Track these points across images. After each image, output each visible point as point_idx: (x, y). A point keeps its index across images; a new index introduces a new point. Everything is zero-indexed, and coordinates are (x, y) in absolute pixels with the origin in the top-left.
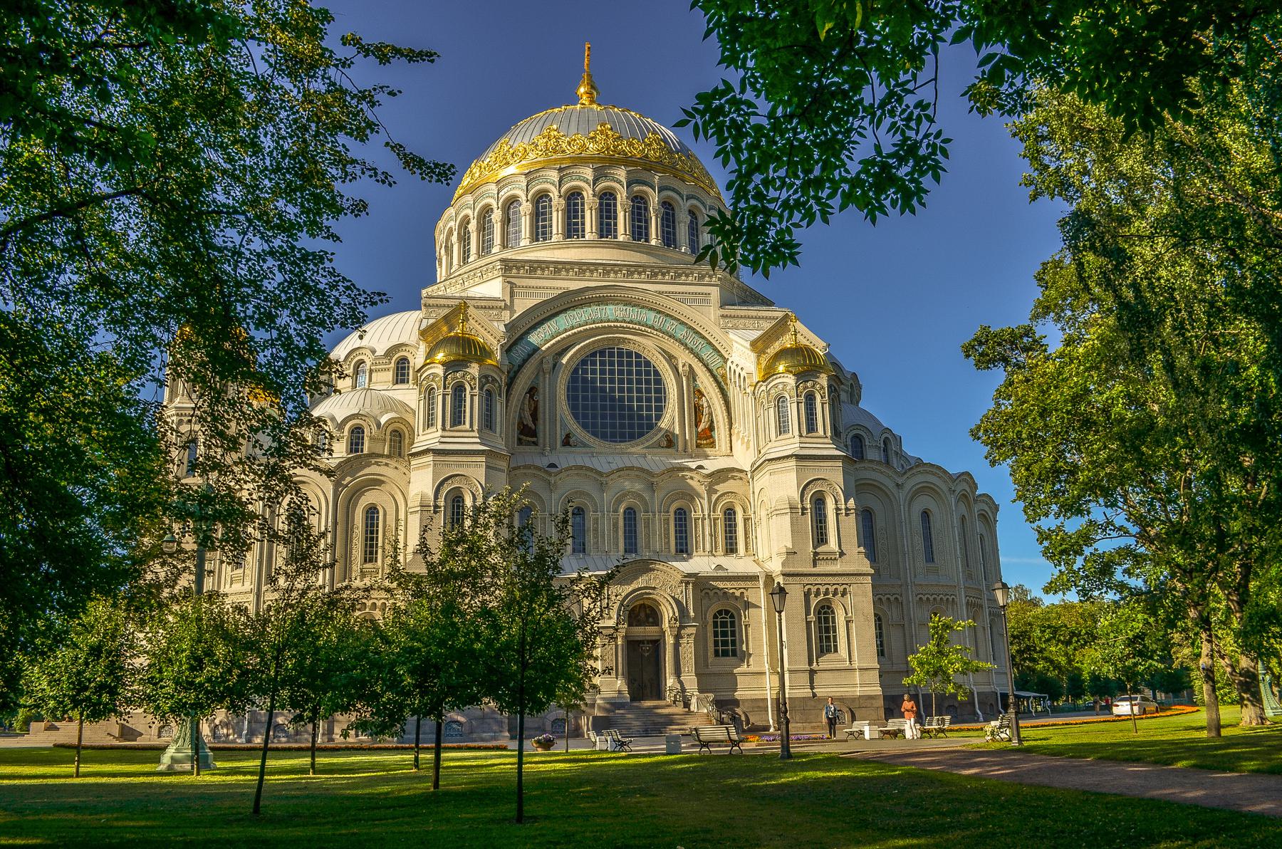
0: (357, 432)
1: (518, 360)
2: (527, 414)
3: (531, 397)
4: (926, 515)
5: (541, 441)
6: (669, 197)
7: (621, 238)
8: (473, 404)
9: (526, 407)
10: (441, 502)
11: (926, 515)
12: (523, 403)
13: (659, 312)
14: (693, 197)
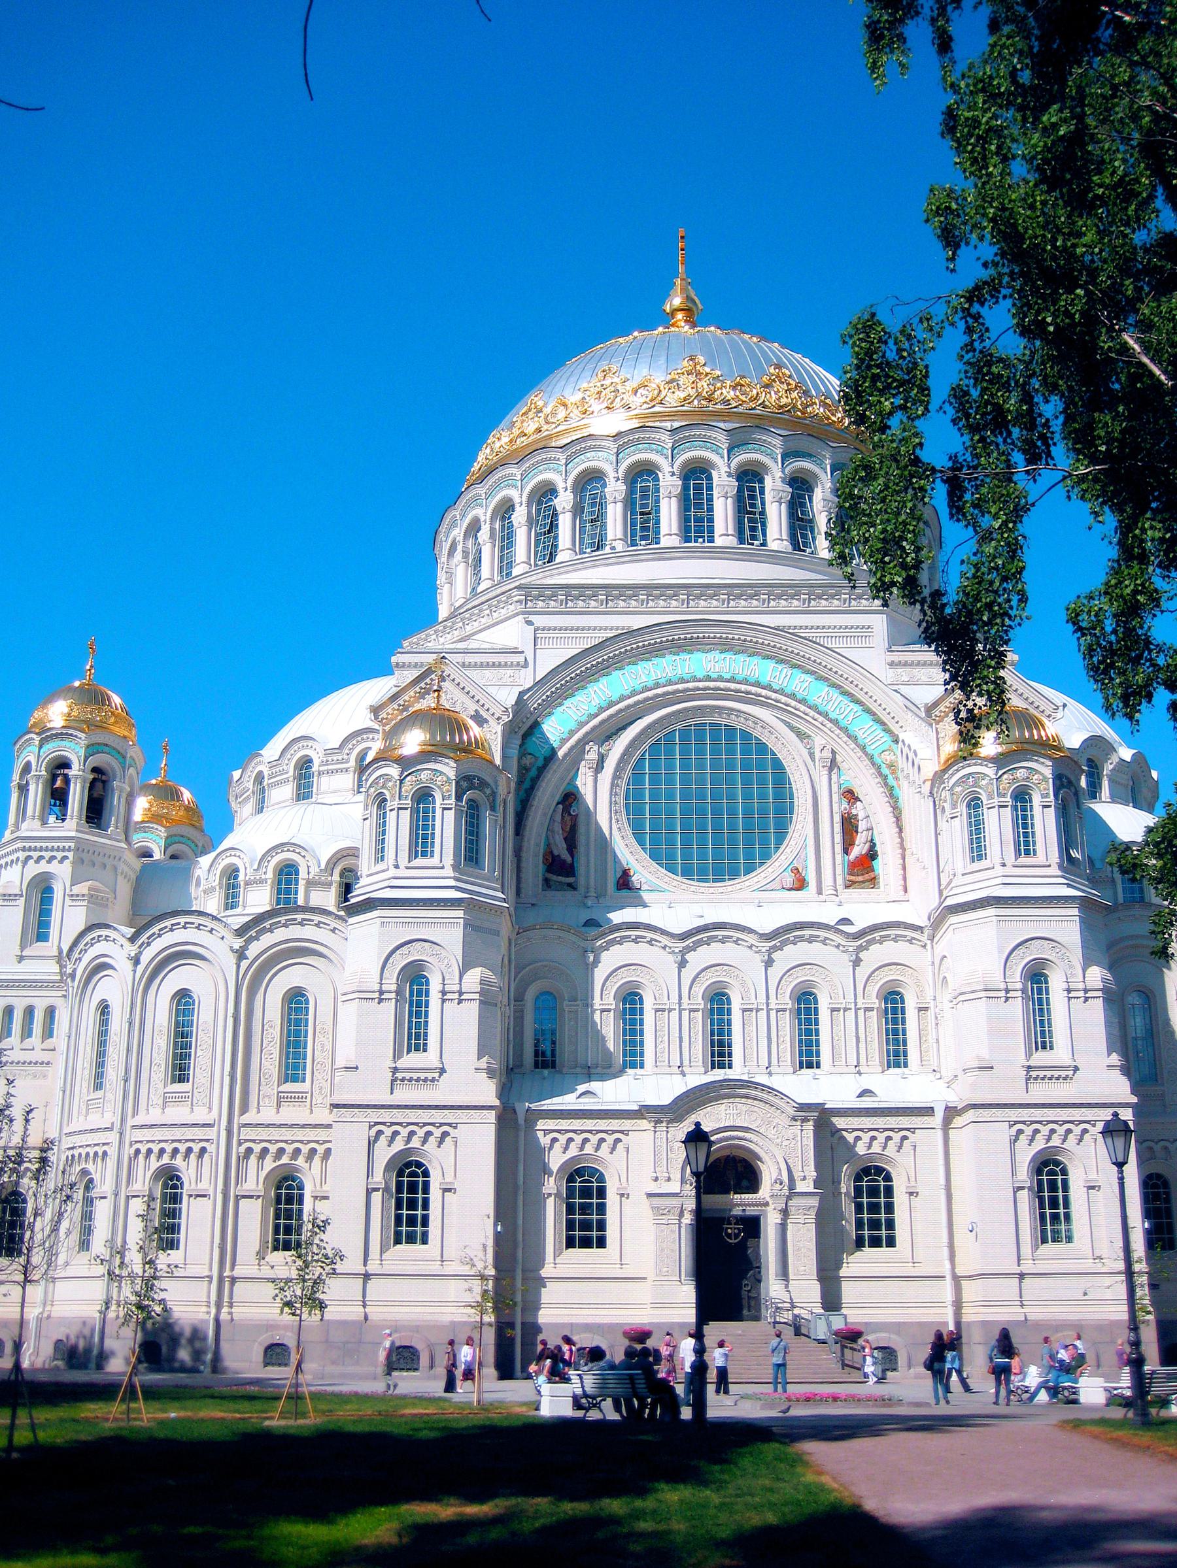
0: (287, 873)
5: (582, 881)
6: (802, 470)
7: (719, 541)
8: (446, 825)
9: (557, 827)
10: (391, 985)
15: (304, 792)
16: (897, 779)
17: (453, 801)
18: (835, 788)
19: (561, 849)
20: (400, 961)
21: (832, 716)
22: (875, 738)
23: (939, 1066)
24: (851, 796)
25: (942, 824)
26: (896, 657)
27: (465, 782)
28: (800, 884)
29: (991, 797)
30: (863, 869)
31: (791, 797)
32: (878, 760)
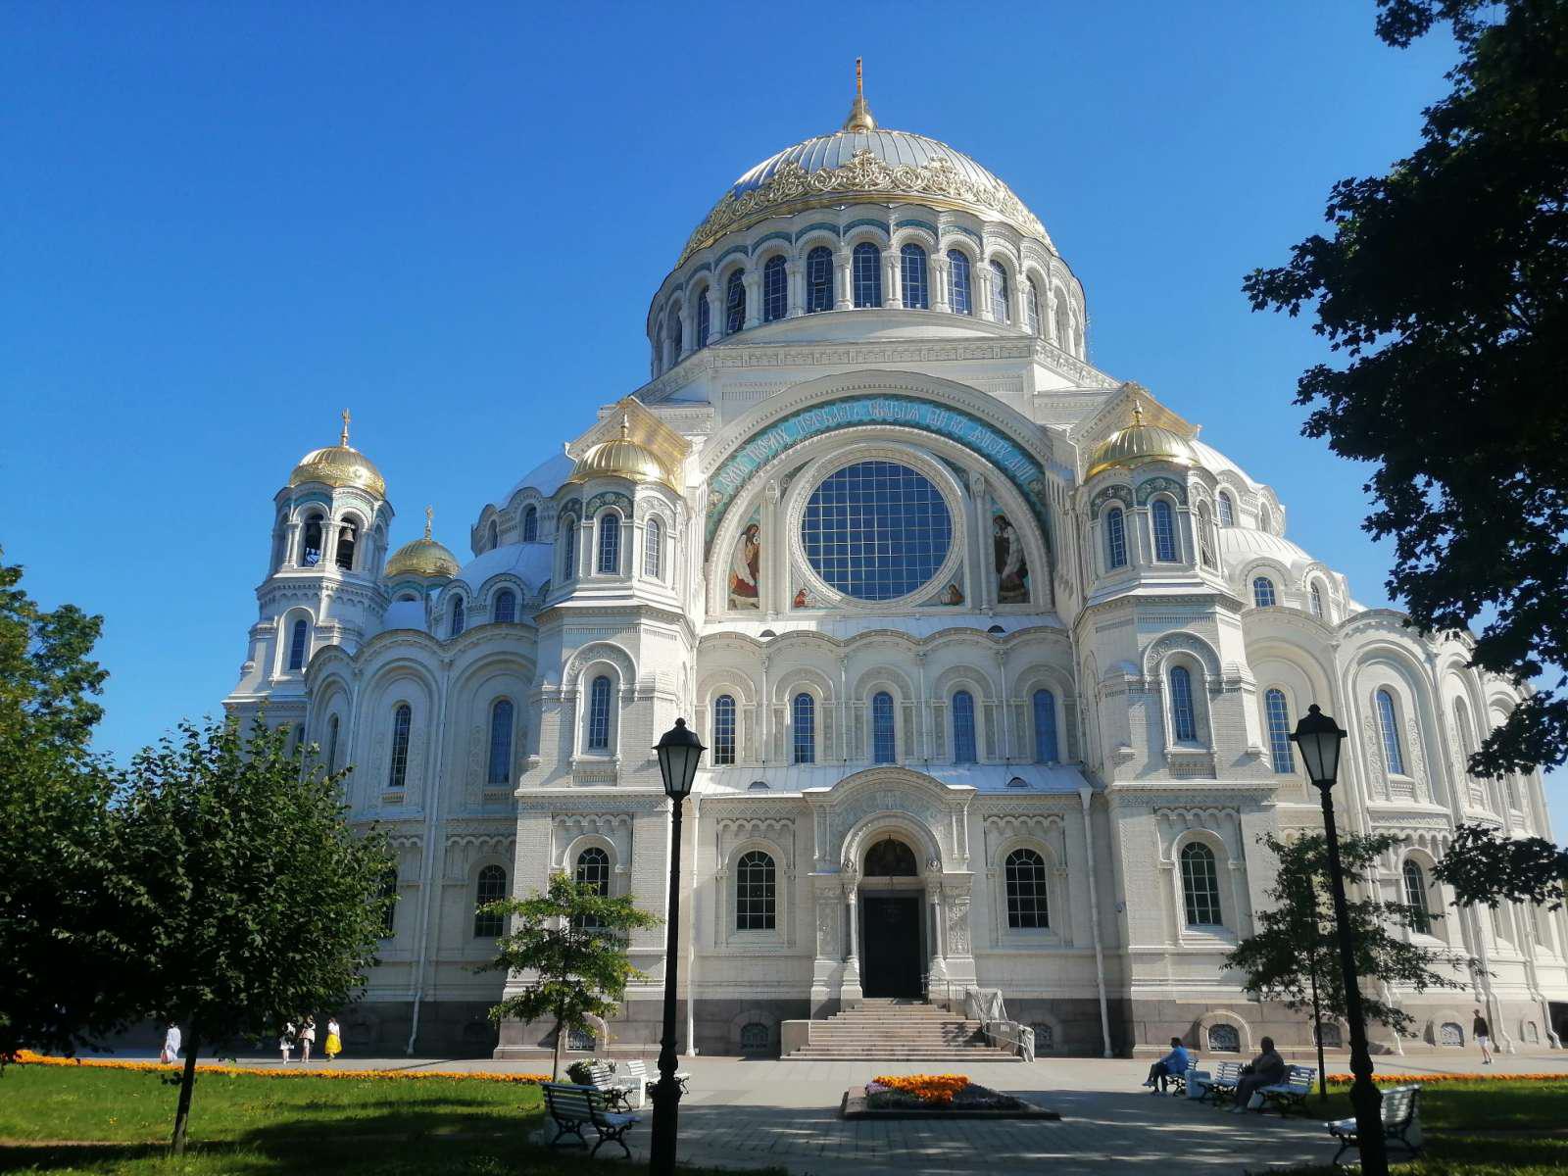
1: (730, 490)
3: (750, 539)
4: (1386, 696)
6: (957, 243)
15: (530, 535)
16: (1044, 505)
18: (989, 515)
19: (744, 574)
21: (986, 451)
23: (1086, 757)
24: (1002, 522)
28: (957, 598)
29: (1129, 505)
30: (1013, 587)
31: (949, 524)
32: (1026, 488)
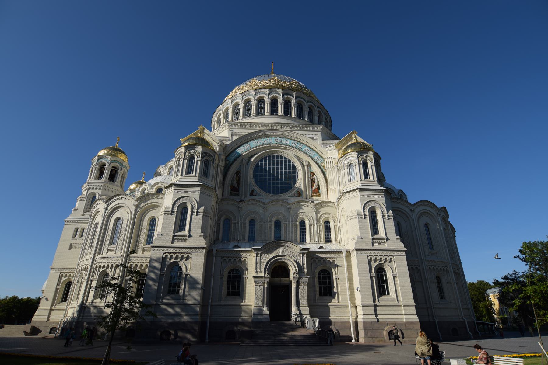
1: (232, 160)
2: (235, 182)
3: (237, 175)
4: (427, 225)
5: (240, 193)
6: (300, 101)
8: (198, 165)
9: (235, 179)
10: (175, 210)
11: (427, 225)
12: (233, 177)
13: (295, 140)
14: (310, 102)
17: (200, 158)
20: (179, 203)
22: (319, 160)
25: (340, 173)
26: (324, 142)
27: (204, 154)
